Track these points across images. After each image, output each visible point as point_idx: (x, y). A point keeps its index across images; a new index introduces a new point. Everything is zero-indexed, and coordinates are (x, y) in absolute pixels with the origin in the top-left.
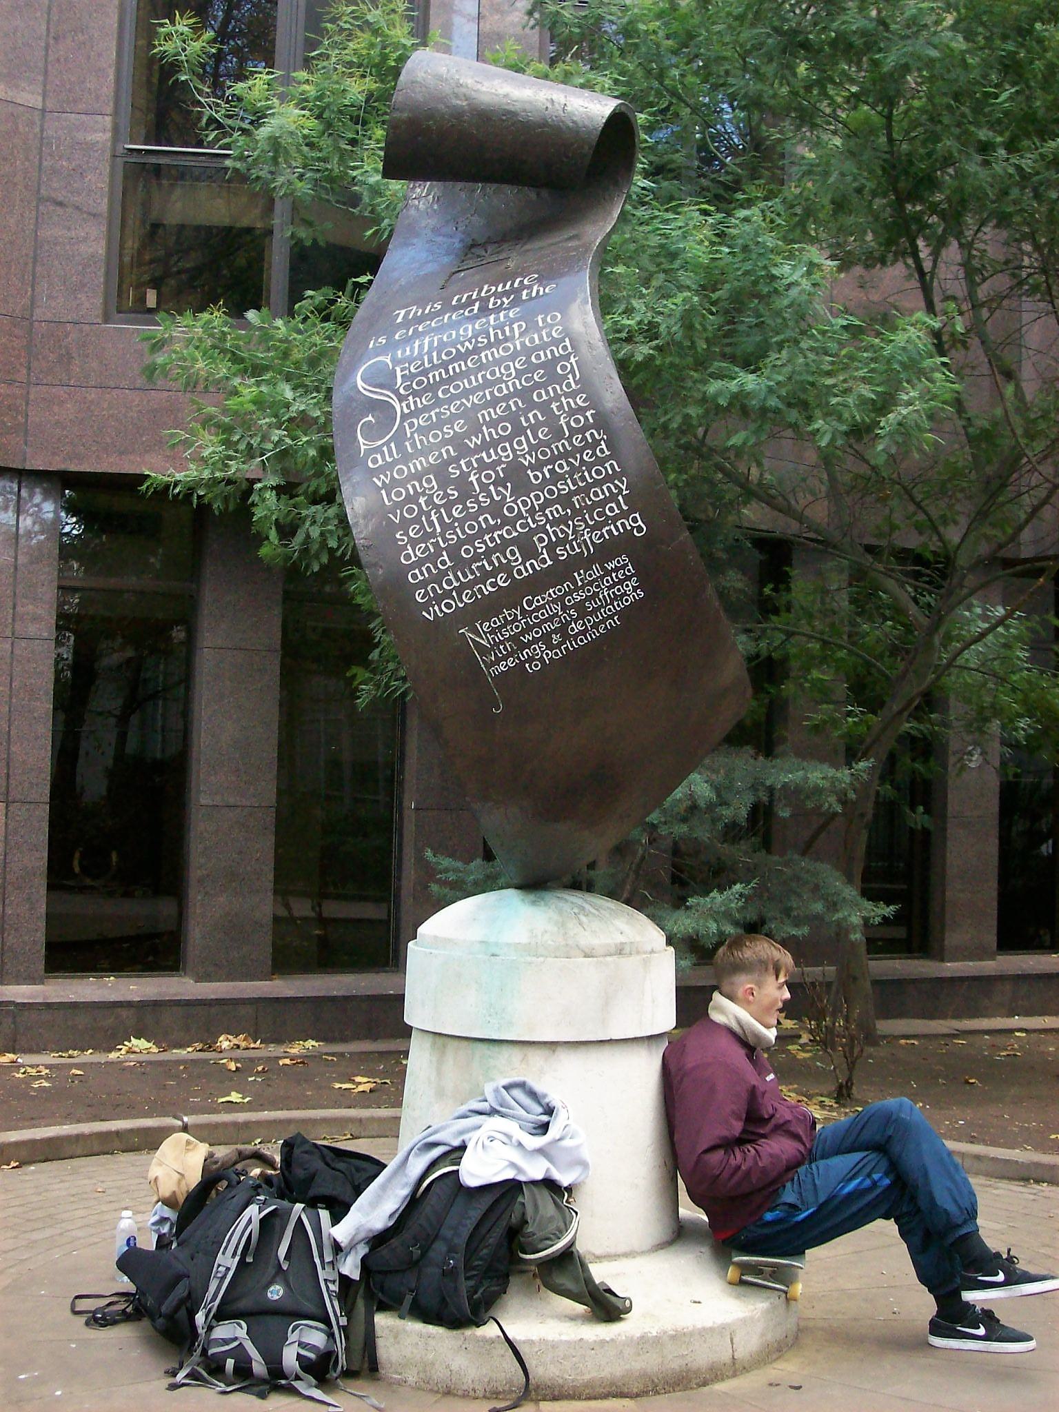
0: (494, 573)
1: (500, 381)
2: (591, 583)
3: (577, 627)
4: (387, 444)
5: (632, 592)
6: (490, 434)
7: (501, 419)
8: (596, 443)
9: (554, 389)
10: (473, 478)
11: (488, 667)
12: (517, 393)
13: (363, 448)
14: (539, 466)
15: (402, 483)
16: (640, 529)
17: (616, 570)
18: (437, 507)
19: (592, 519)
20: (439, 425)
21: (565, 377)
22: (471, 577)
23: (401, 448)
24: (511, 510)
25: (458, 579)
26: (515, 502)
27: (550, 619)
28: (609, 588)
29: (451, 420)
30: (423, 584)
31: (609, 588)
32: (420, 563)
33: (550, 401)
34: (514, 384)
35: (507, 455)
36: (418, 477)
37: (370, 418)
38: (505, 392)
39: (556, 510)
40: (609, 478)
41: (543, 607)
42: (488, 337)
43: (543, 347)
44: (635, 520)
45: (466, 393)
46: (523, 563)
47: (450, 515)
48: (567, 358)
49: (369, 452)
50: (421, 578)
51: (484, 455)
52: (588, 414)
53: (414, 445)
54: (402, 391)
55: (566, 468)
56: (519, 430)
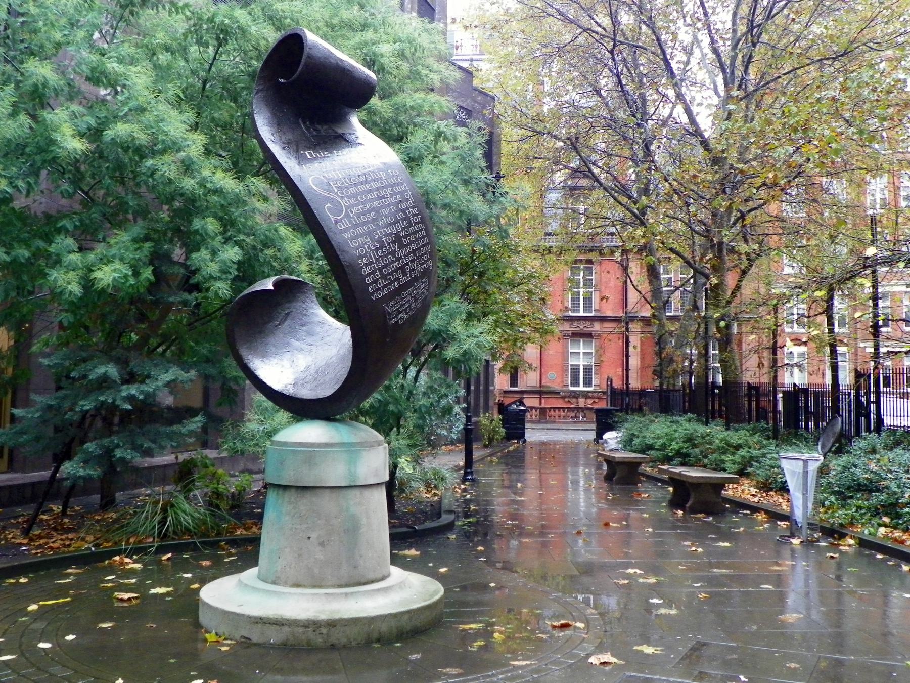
8: (421, 230)
14: (406, 237)
30: (371, 284)
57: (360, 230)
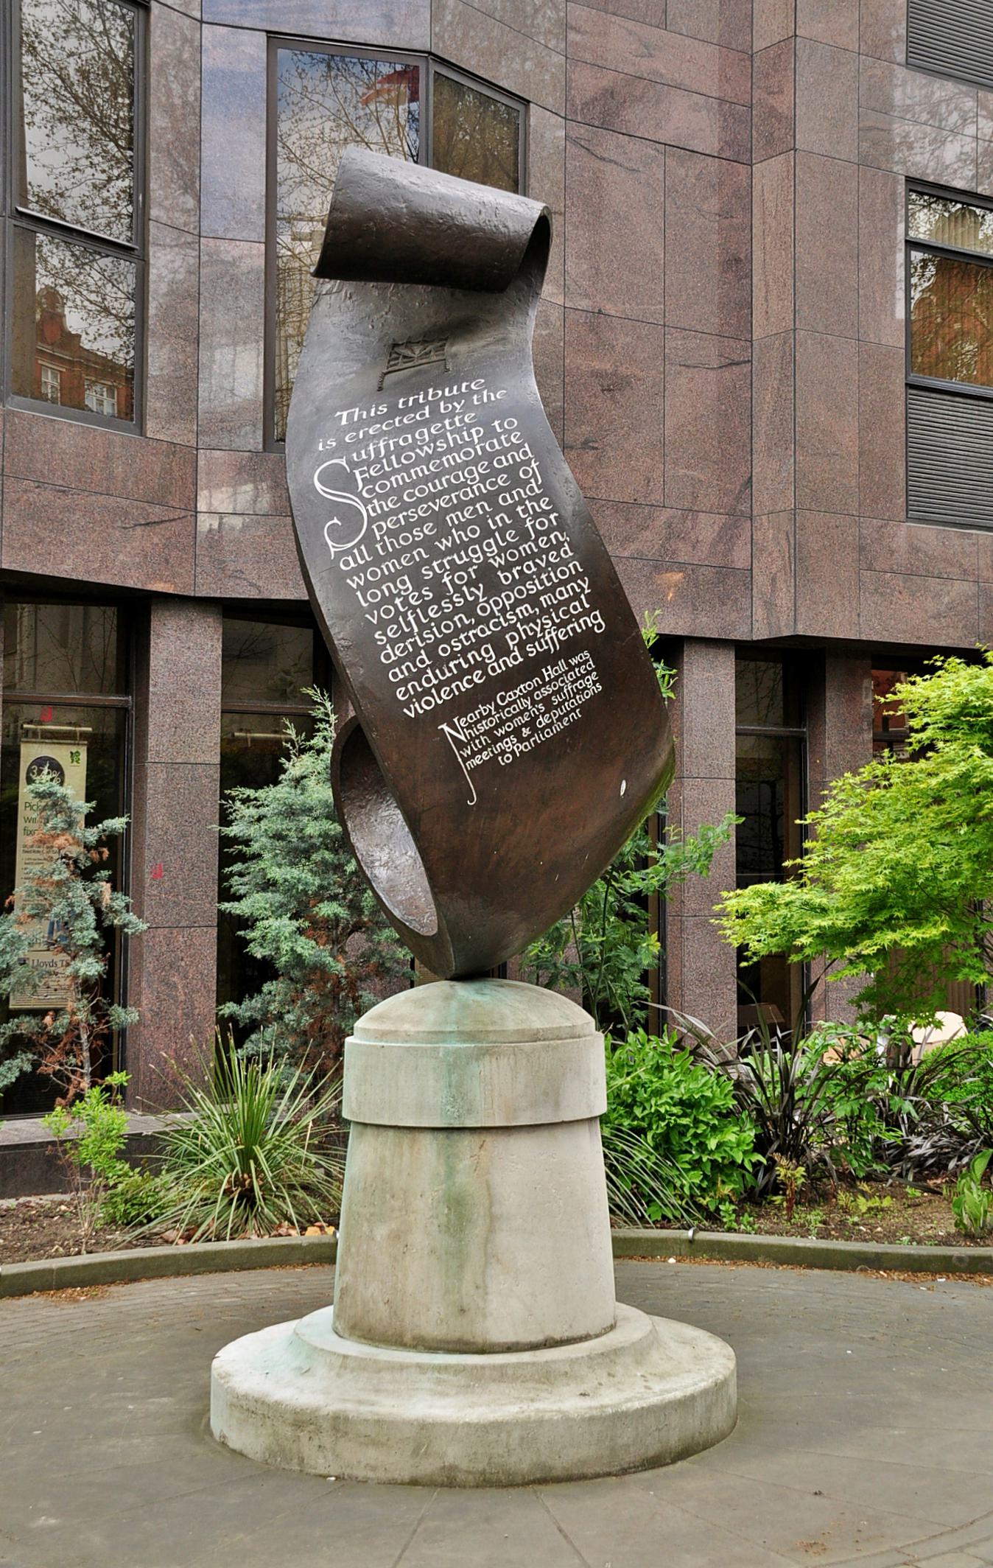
0: (470, 671)
1: (465, 485)
2: (556, 679)
3: (544, 721)
4: (358, 546)
5: (592, 686)
6: (460, 536)
7: (469, 522)
8: (560, 544)
9: (518, 493)
10: (446, 580)
11: (465, 760)
12: (482, 497)
13: (332, 550)
14: (507, 567)
15: (378, 585)
16: (600, 626)
17: (579, 665)
18: (414, 608)
19: (558, 617)
20: (409, 527)
21: (528, 482)
22: (448, 675)
23: (373, 551)
24: (484, 610)
25: (436, 677)
26: (487, 602)
27: (521, 713)
28: (573, 682)
29: (421, 522)
30: (404, 682)
31: (573, 682)
32: (399, 662)
33: (515, 505)
34: (479, 488)
35: (477, 558)
36: (392, 578)
37: (336, 521)
38: (471, 496)
39: (525, 610)
40: (572, 578)
41: (514, 702)
42: (447, 441)
43: (504, 452)
44: (595, 618)
45: (433, 497)
46: (497, 660)
47: (426, 616)
48: (528, 463)
49: (340, 555)
50: (401, 676)
51: (455, 557)
52: (552, 517)
53: (384, 547)
54: (365, 494)
55: (534, 569)
56: (487, 533)
57: (390, 566)
